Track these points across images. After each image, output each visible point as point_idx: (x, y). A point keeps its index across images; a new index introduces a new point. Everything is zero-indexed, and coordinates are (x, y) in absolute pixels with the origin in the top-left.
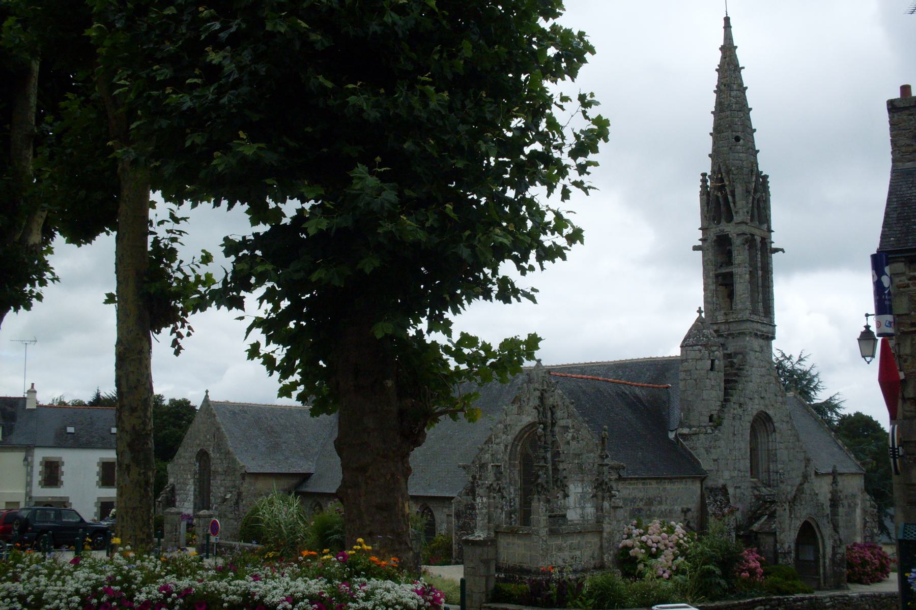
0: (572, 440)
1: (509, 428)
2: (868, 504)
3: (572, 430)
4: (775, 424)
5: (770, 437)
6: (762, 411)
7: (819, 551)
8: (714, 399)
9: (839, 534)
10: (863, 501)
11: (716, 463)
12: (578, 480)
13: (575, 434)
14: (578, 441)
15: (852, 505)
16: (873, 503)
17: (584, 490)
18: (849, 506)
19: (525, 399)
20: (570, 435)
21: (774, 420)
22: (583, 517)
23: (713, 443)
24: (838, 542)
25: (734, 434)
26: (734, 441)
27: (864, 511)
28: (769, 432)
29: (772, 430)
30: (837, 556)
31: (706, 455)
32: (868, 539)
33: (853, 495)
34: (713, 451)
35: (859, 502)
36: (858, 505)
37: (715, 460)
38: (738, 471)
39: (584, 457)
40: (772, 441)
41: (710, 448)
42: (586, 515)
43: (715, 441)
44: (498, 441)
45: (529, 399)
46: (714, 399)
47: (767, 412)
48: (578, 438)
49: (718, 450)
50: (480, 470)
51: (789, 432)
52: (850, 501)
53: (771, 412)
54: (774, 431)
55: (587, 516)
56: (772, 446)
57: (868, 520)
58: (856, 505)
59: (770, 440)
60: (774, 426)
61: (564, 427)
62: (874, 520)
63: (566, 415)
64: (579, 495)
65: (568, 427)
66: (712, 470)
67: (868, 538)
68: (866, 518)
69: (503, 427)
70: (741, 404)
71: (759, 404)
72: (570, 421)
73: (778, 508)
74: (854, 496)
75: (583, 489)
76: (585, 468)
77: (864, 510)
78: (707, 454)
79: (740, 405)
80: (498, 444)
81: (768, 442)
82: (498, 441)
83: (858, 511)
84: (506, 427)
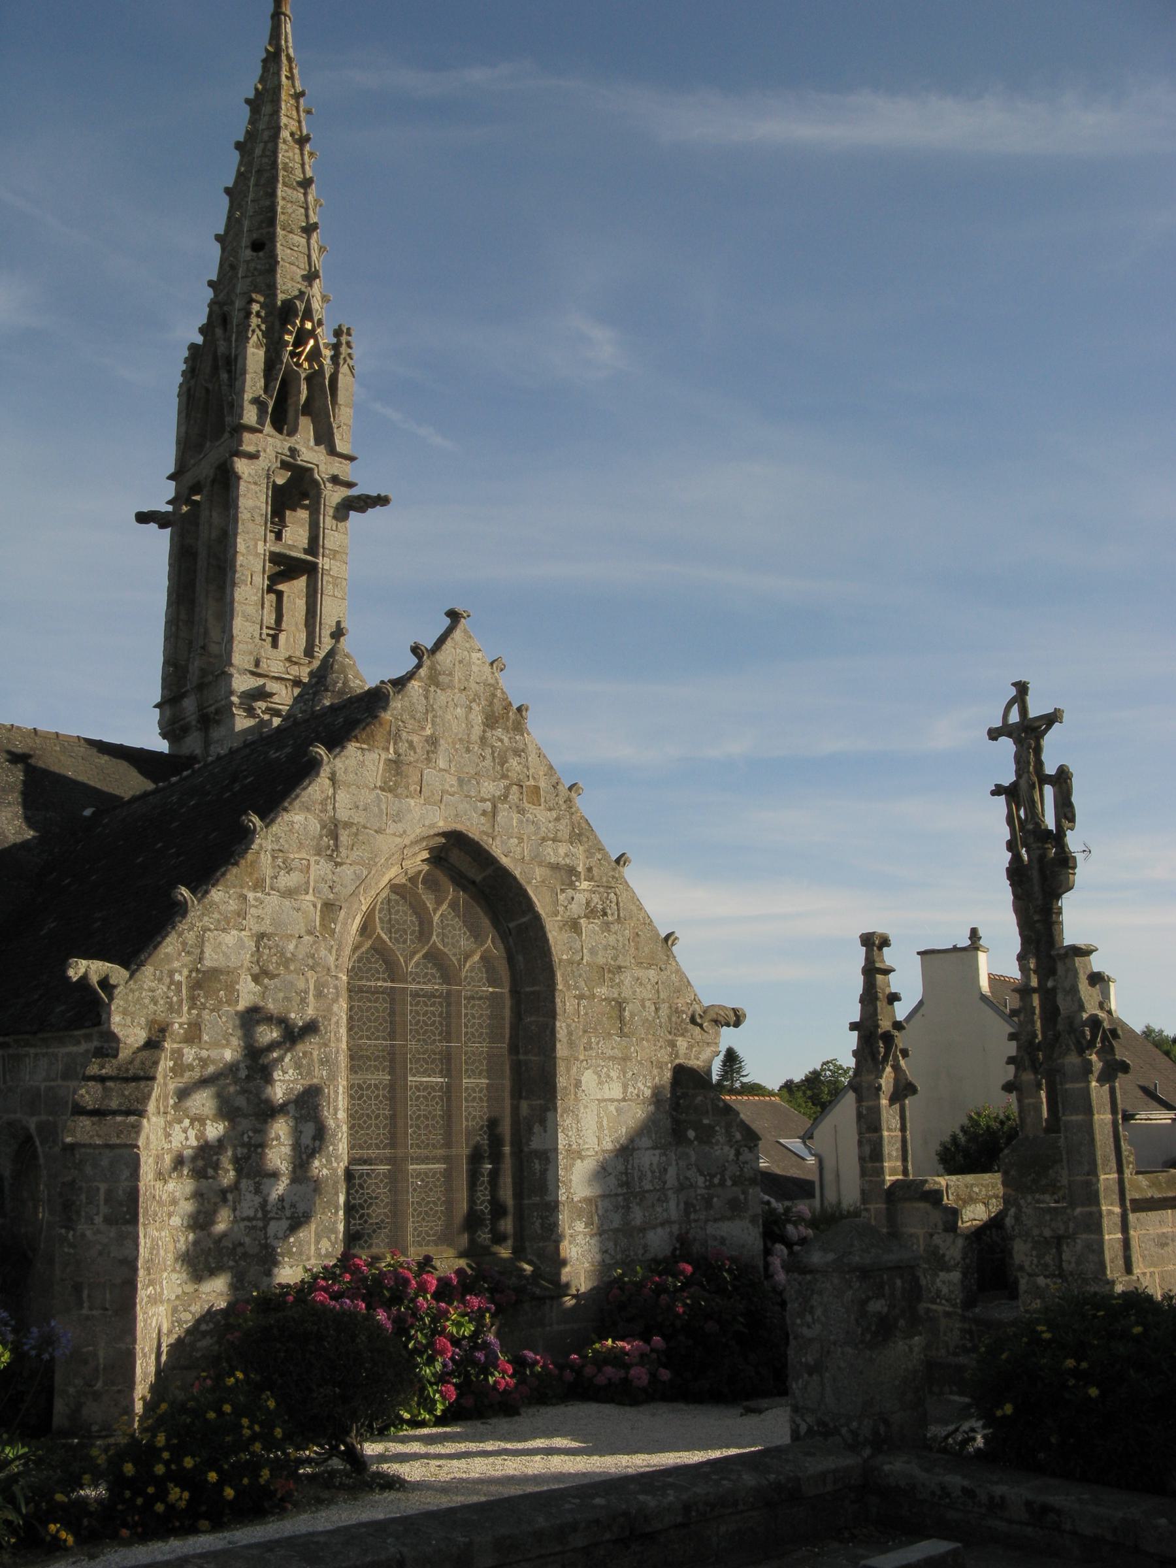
0: (586, 916)
1: (344, 837)
3: (585, 885)
12: (613, 1058)
13: (596, 898)
14: (607, 924)
17: (630, 1089)
19: (415, 739)
20: (581, 898)
22: (626, 1184)
39: (627, 978)
42: (636, 1174)
44: (286, 880)
45: (433, 741)
48: (605, 914)
50: (193, 999)
55: (640, 1179)
61: (555, 867)
63: (564, 829)
64: (612, 1108)
65: (572, 871)
69: (315, 826)
72: (579, 851)
75: (625, 1087)
76: (632, 1015)
80: (289, 893)
82: (286, 880)
84: (333, 829)
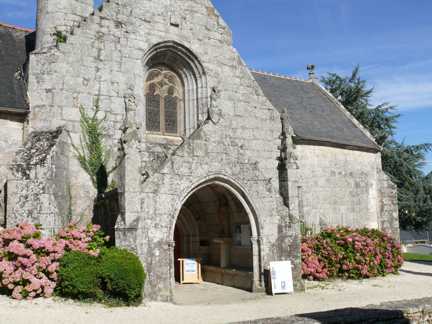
2: (386, 184)
4: (205, 65)
5: (199, 82)
6: (174, 42)
7: (251, 235)
8: (64, 11)
9: (288, 207)
10: (380, 181)
11: (50, 94)
15: (362, 184)
16: (391, 183)
18: (357, 185)
21: (202, 58)
23: (46, 66)
24: (287, 220)
25: (98, 58)
26: (98, 70)
27: (381, 193)
28: (198, 76)
29: (201, 72)
30: (286, 240)
31: (36, 85)
32: (386, 225)
33: (362, 173)
34: (46, 77)
35: (374, 183)
36: (372, 185)
37: (48, 91)
38: (106, 111)
40: (202, 87)
41: (43, 74)
43: (49, 64)
46: (64, 11)
47: (186, 45)
49: (54, 76)
51: (238, 80)
52: (358, 180)
53: (195, 47)
54: (204, 73)
56: (202, 94)
57: (385, 203)
58: (368, 185)
59: (199, 85)
60: (202, 67)
62: (393, 203)
66: (44, 106)
67: (386, 223)
68: (383, 201)
70: (120, 23)
71: (167, 31)
73: (148, 159)
74: (364, 174)
77: (381, 191)
78: (38, 82)
79: (119, 24)
81: (197, 88)
83: (373, 193)
